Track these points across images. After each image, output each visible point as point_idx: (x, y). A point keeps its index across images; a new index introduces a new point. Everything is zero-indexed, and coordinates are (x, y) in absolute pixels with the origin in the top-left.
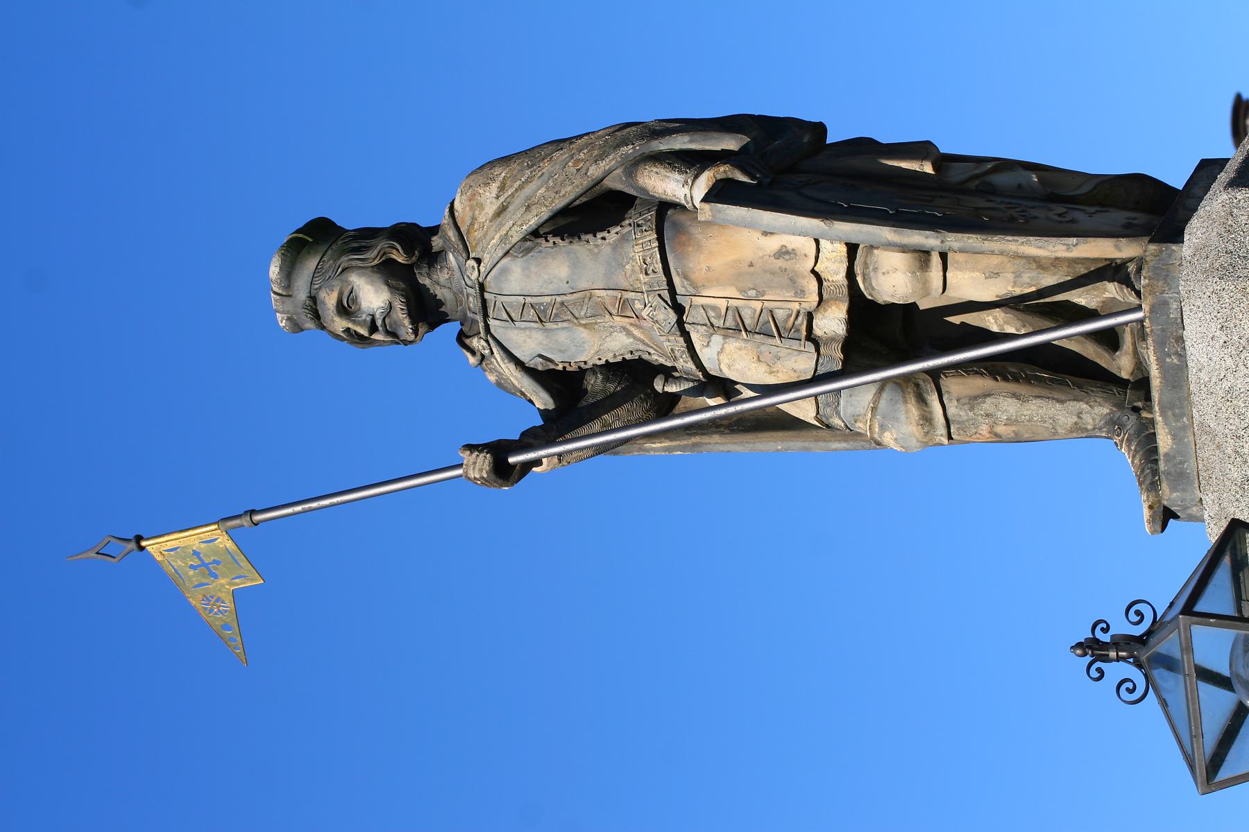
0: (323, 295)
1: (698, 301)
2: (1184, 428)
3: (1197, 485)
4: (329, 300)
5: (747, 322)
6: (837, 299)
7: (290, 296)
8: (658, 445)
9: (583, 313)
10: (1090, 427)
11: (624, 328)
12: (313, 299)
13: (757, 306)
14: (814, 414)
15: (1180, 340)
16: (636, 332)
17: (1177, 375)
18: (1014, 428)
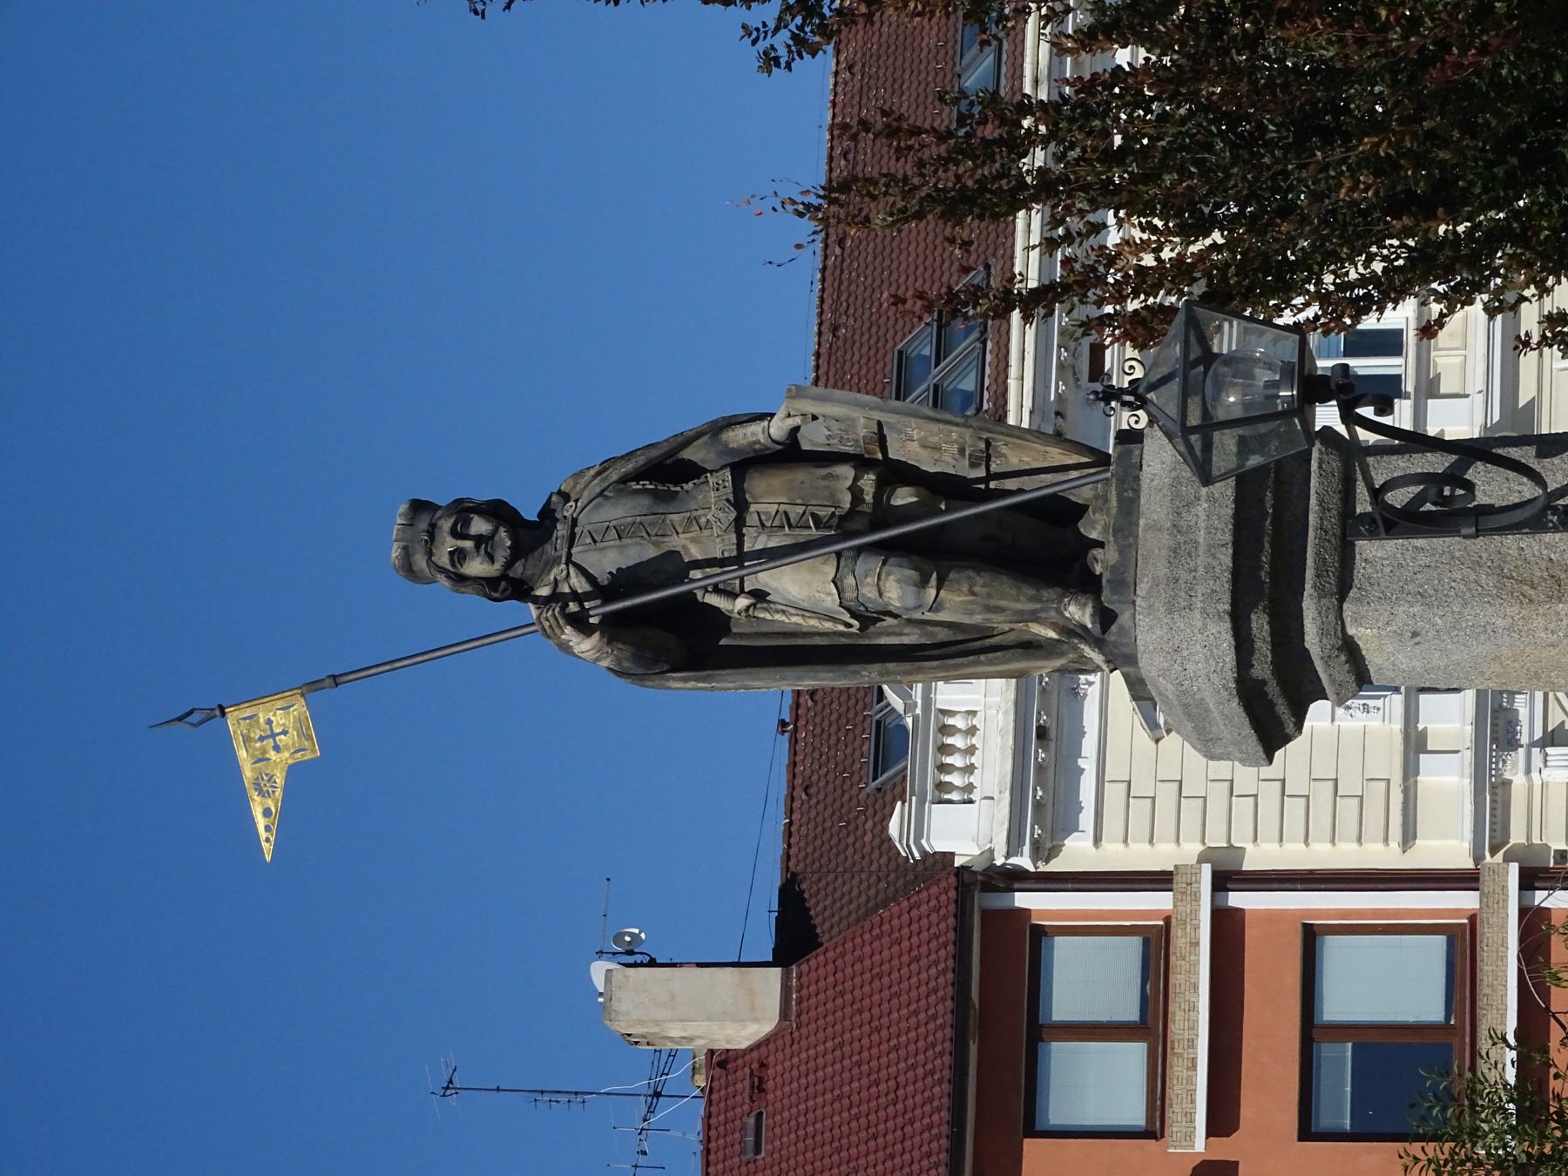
0: (440, 523)
2: (1130, 546)
3: (1132, 589)
5: (792, 521)
7: (411, 525)
8: (678, 675)
9: (654, 533)
10: (1045, 599)
13: (800, 510)
14: (832, 575)
15: (1137, 479)
18: (988, 590)
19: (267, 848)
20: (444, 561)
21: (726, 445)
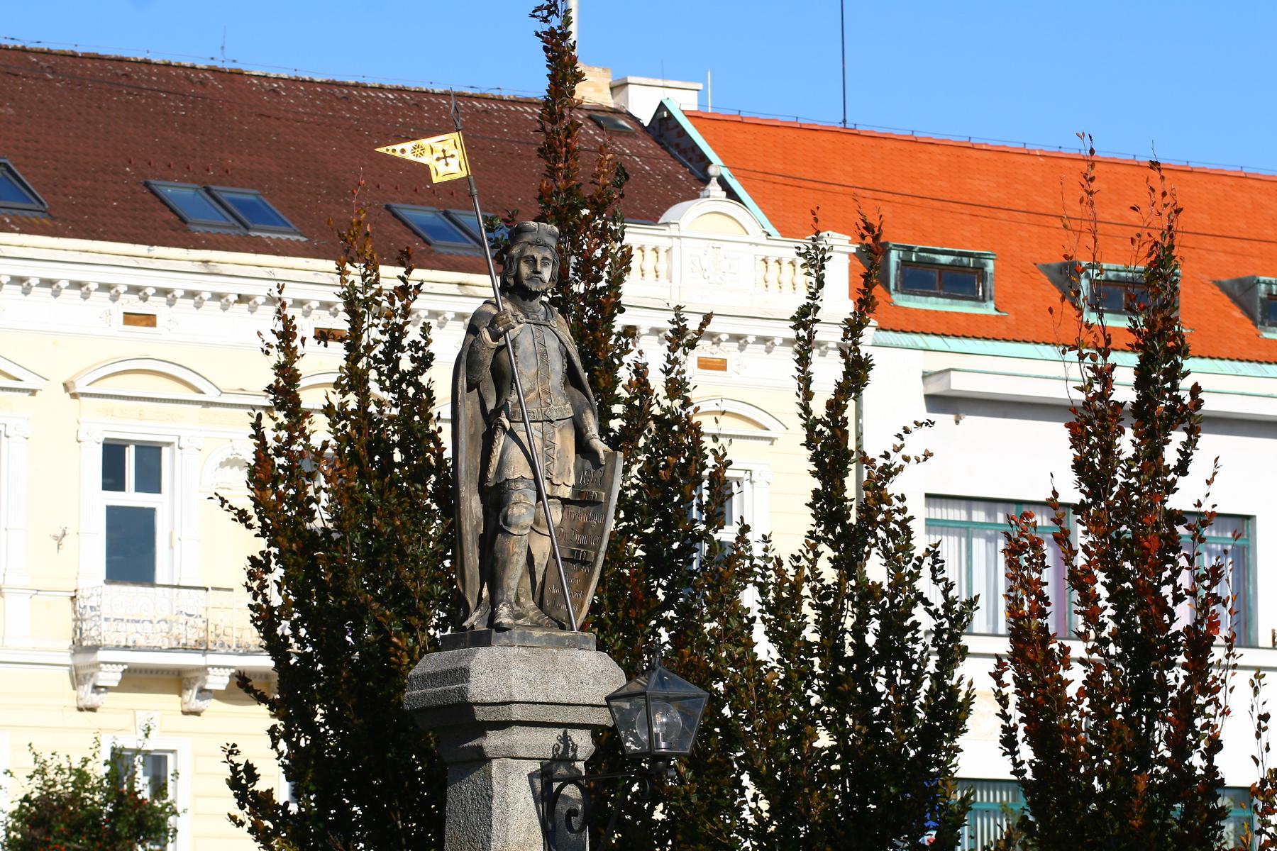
1: (556, 430)
4: (548, 254)
6: (552, 490)
11: (534, 389)
12: (546, 246)
16: (533, 395)
17: (560, 643)
19: (382, 150)
20: (528, 253)
21: (584, 412)
